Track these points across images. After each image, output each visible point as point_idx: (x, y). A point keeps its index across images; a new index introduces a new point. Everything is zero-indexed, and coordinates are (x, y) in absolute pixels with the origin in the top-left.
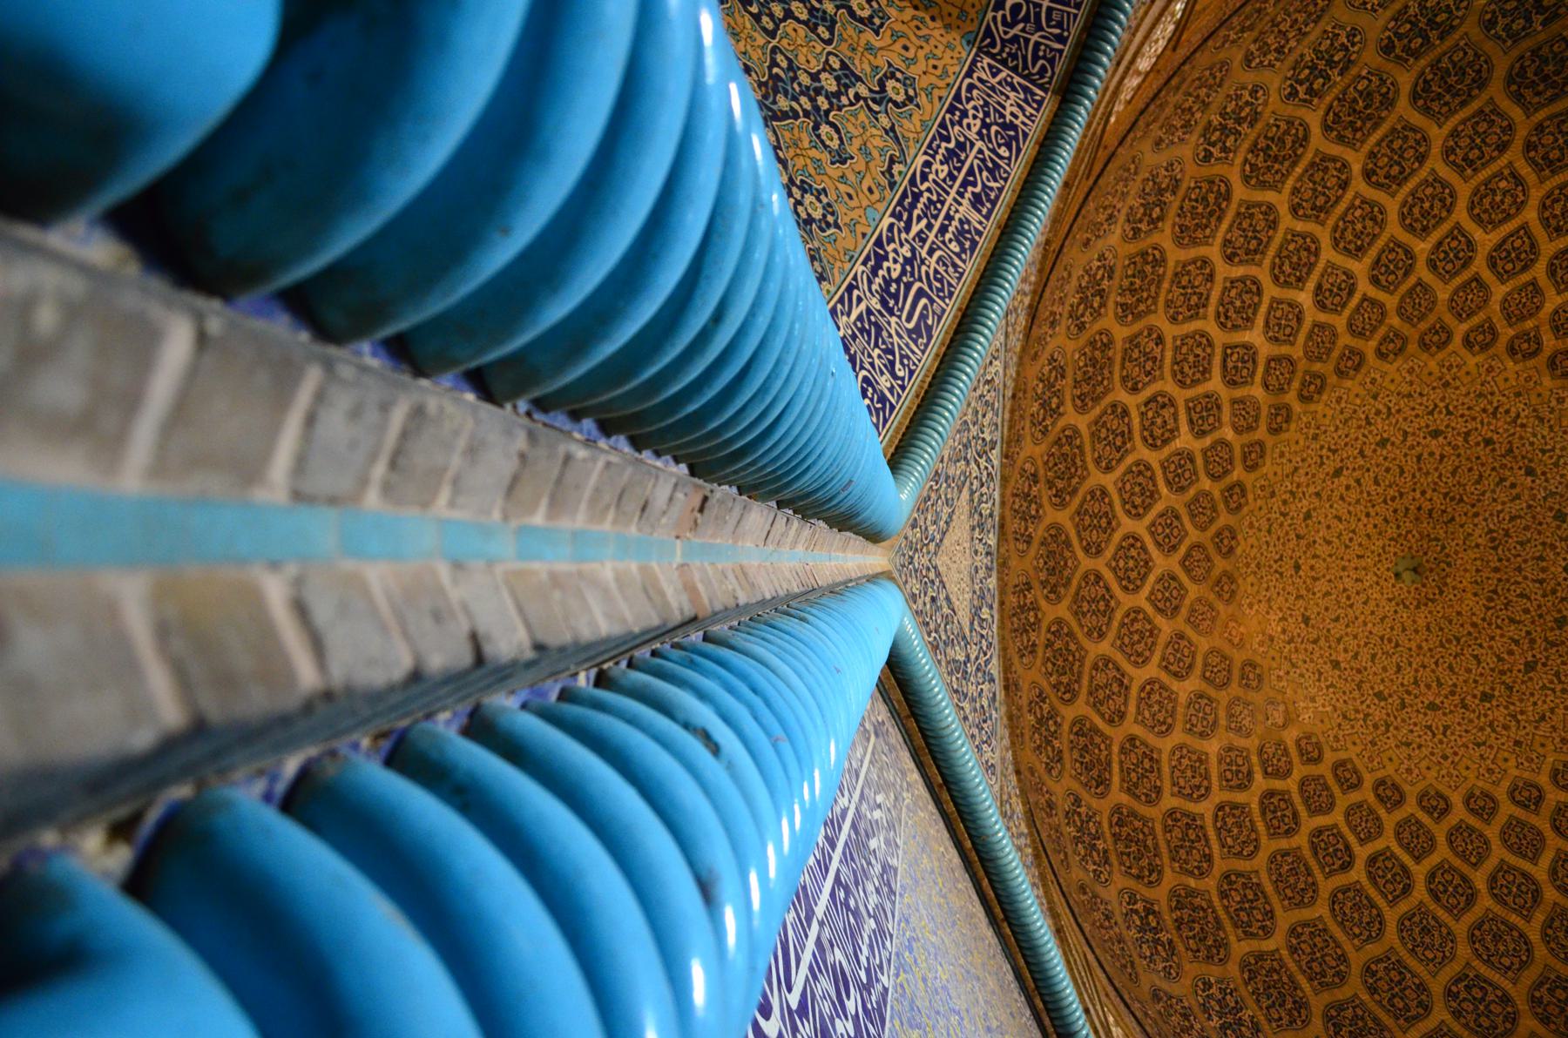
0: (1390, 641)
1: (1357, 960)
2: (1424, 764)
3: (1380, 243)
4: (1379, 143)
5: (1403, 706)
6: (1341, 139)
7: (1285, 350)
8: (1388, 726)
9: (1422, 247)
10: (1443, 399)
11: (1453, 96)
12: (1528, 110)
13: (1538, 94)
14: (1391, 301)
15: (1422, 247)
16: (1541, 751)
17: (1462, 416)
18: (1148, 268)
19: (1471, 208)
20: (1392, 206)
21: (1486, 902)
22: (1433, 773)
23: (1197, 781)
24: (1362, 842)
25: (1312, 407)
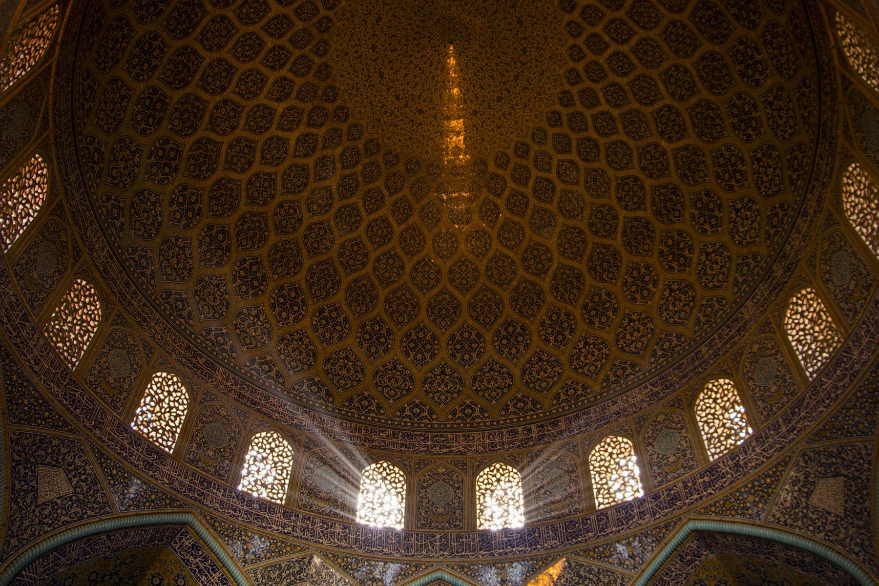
0: (478, 71)
1: (583, 226)
2: (537, 106)
3: (262, 69)
4: (207, 91)
5: (509, 91)
6: (202, 117)
7: (305, 116)
8: (513, 108)
9: (270, 43)
10: (360, 17)
11: (189, 60)
12: (205, 12)
13: (196, 16)
14: (297, 53)
15: (270, 43)
16: (558, 52)
17: (373, 7)
18: (245, 227)
19: (255, 23)
20: (243, 67)
21: (602, 141)
22: (543, 106)
23: (484, 241)
24: (549, 171)
25: (341, 92)
